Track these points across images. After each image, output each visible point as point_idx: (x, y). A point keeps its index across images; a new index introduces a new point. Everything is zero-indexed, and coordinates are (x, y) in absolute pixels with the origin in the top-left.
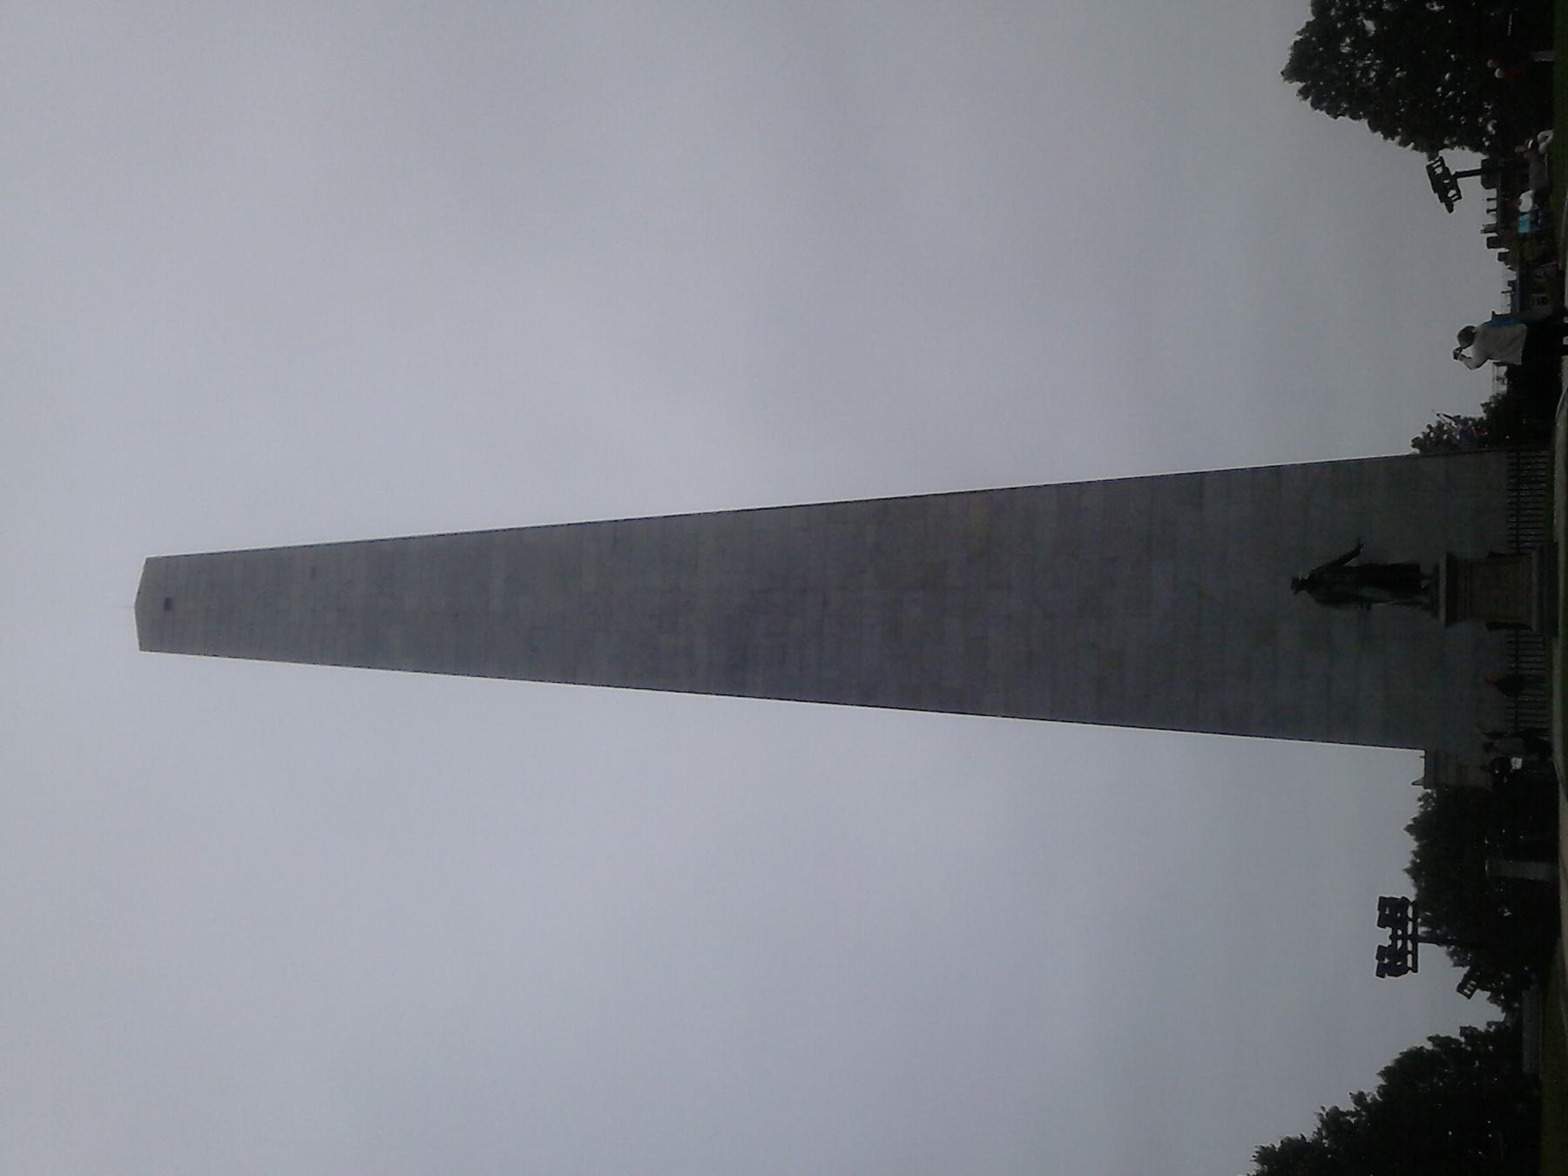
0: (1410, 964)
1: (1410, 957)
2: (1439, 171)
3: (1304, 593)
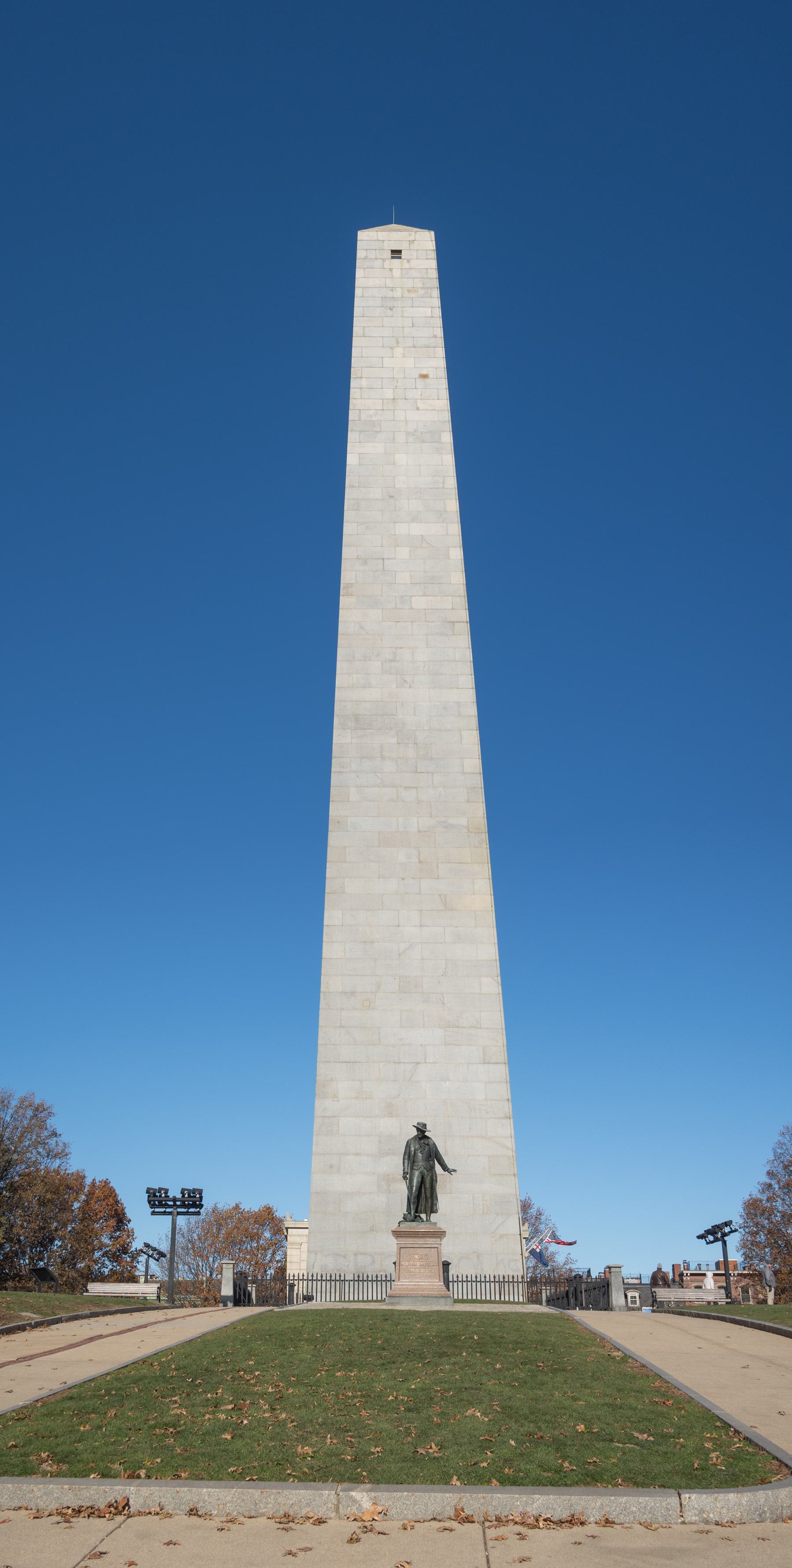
0: (157, 1210)
1: (162, 1210)
2: (727, 1229)
3: (414, 1133)
